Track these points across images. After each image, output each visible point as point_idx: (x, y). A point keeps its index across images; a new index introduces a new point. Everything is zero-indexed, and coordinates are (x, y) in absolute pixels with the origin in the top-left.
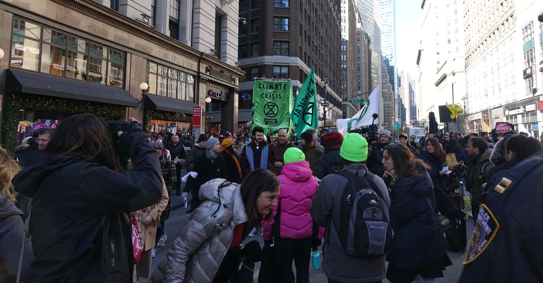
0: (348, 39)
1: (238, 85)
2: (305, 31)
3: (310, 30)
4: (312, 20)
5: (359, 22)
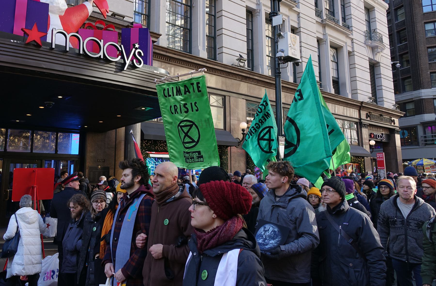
1: (398, 125)
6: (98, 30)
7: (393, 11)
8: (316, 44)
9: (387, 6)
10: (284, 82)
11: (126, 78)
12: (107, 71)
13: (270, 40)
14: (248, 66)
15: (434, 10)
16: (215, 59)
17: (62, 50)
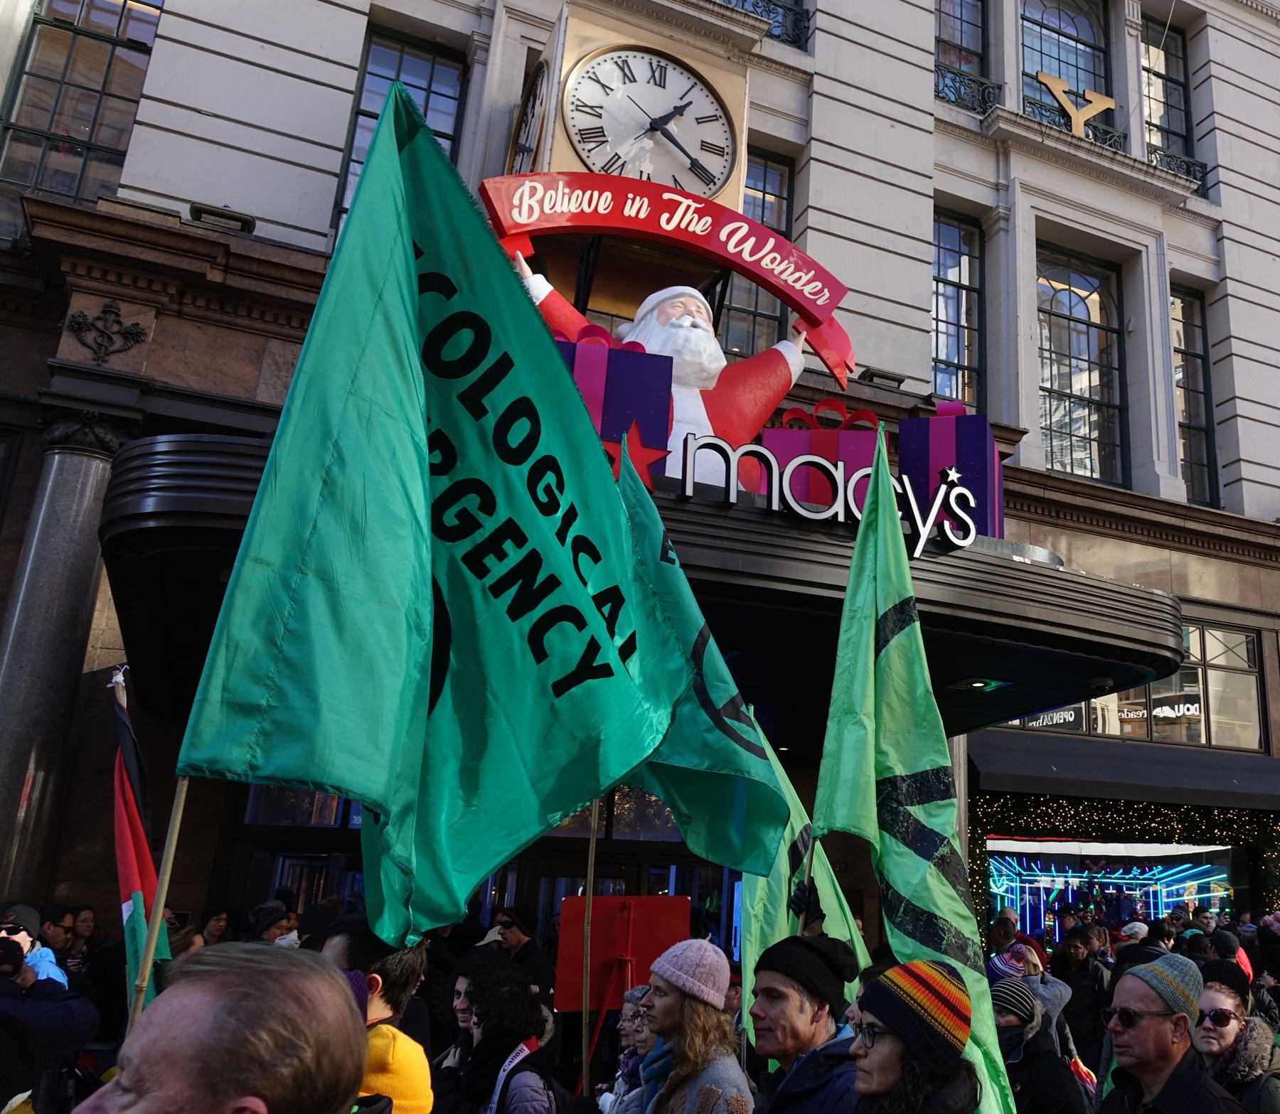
6: (823, 431)
16: (1215, 503)
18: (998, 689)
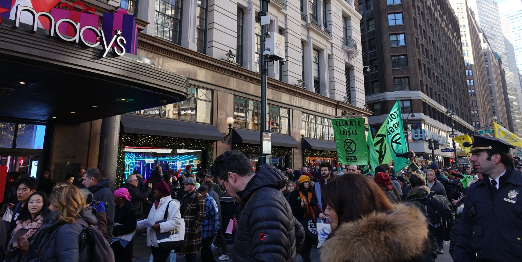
0: (473, 63)
2: (424, 64)
3: (429, 63)
4: (430, 53)
5: (484, 42)
6: (75, 12)
7: (366, 21)
8: (301, 46)
9: (361, 16)
10: (270, 79)
11: (105, 67)
12: (82, 58)
13: (259, 37)
14: (238, 62)
15: (397, 24)
16: (205, 52)
17: (28, 29)
18: (131, 101)
